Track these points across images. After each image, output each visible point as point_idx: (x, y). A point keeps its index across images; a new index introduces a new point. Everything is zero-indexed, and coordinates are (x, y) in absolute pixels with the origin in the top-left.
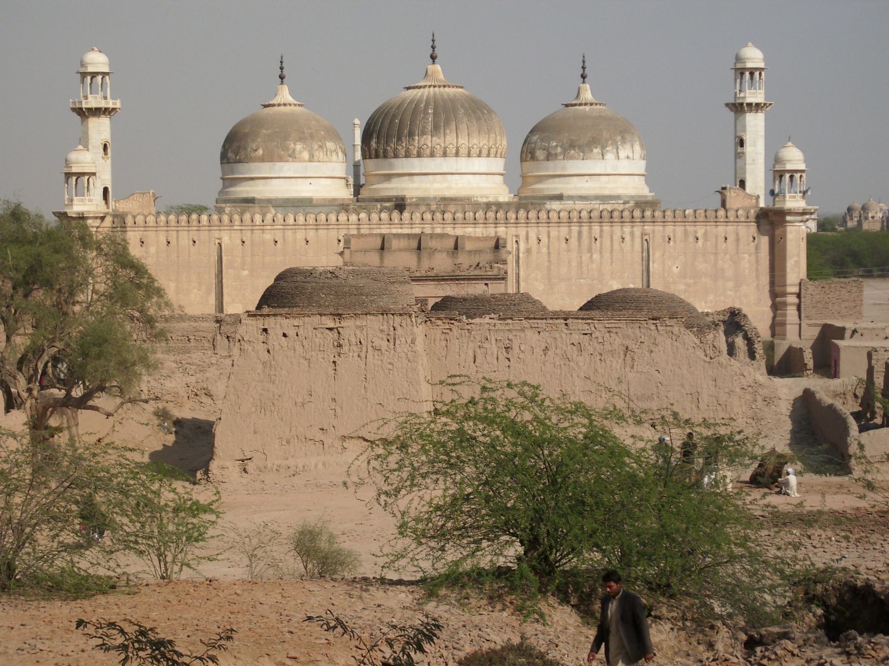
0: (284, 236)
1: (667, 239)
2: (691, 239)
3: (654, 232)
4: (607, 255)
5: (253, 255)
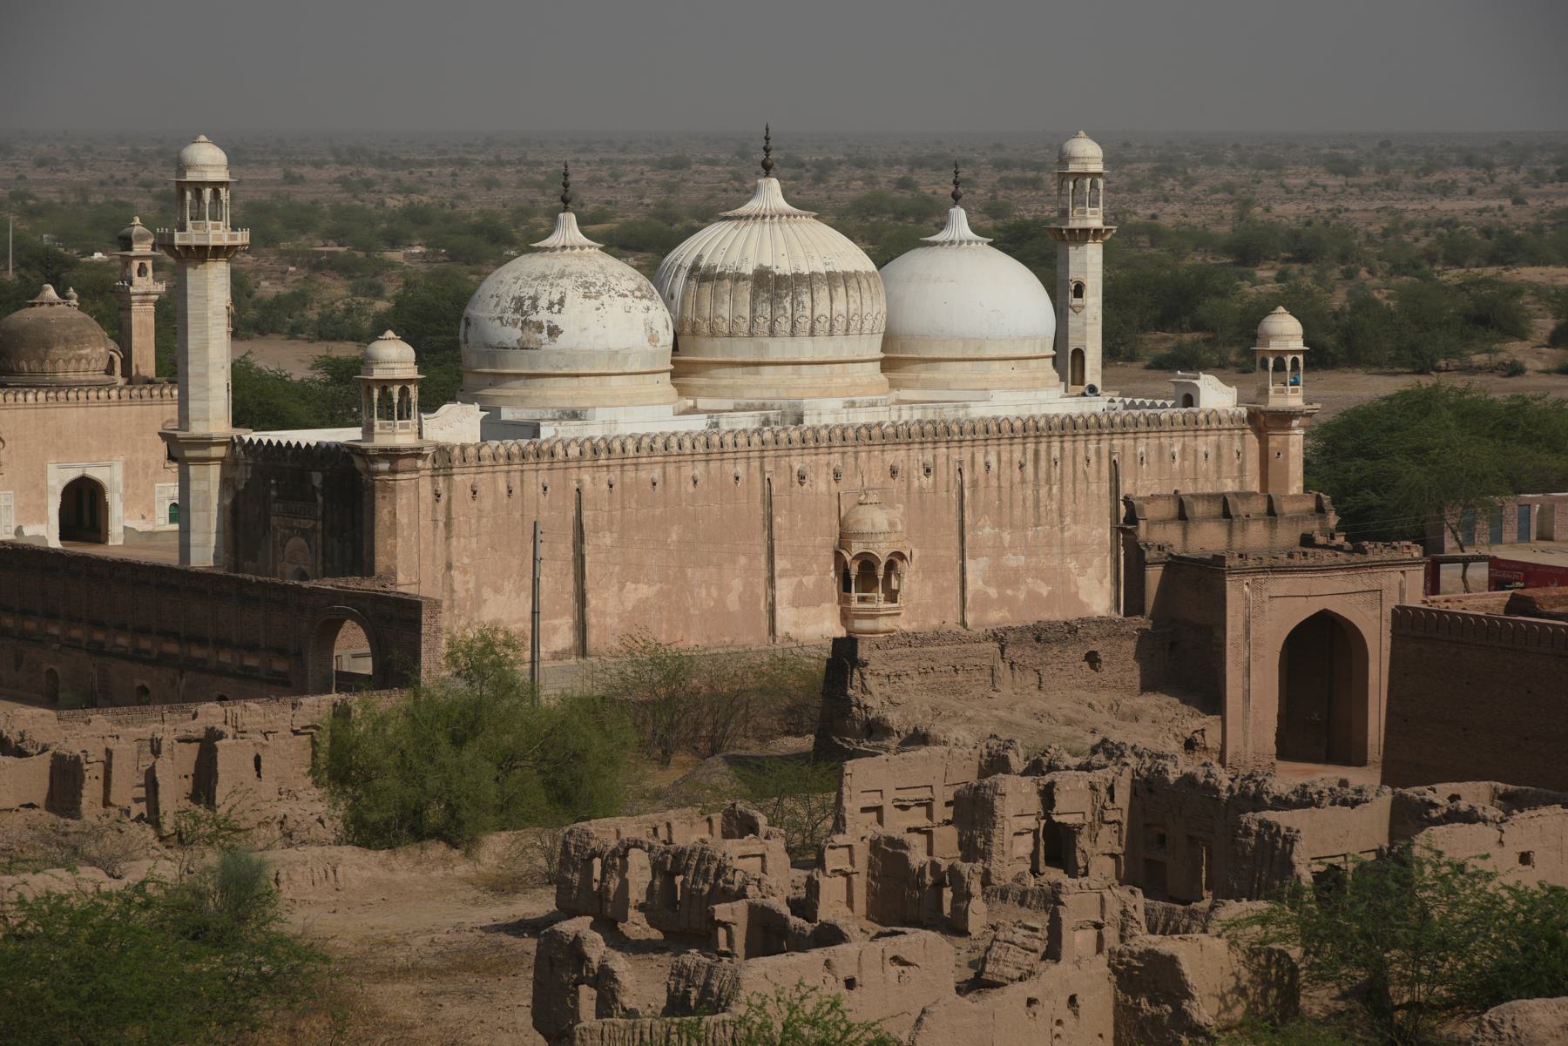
2: (1167, 457)
4: (1069, 487)
5: (623, 508)
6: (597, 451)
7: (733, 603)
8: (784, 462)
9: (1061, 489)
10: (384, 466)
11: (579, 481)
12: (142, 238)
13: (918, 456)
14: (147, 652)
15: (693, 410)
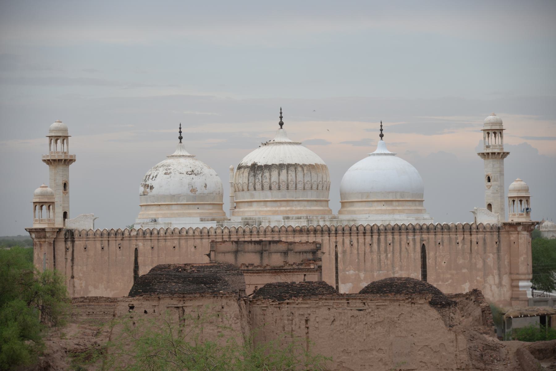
0: (179, 243)
1: (438, 244)
2: (454, 243)
3: (428, 238)
4: (397, 255)
5: (159, 256)
11: (136, 245)
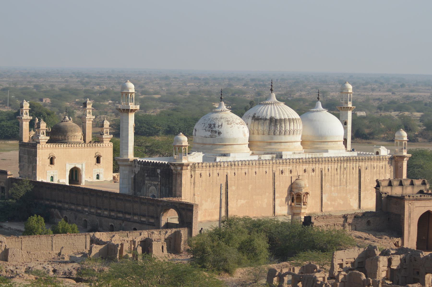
2: (373, 168)
6: (232, 164)
7: (265, 205)
8: (278, 168)
9: (346, 176)
10: (179, 168)
12: (89, 104)
13: (309, 167)
14: (113, 216)
15: (253, 154)
